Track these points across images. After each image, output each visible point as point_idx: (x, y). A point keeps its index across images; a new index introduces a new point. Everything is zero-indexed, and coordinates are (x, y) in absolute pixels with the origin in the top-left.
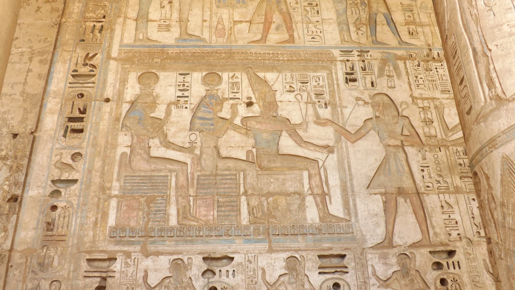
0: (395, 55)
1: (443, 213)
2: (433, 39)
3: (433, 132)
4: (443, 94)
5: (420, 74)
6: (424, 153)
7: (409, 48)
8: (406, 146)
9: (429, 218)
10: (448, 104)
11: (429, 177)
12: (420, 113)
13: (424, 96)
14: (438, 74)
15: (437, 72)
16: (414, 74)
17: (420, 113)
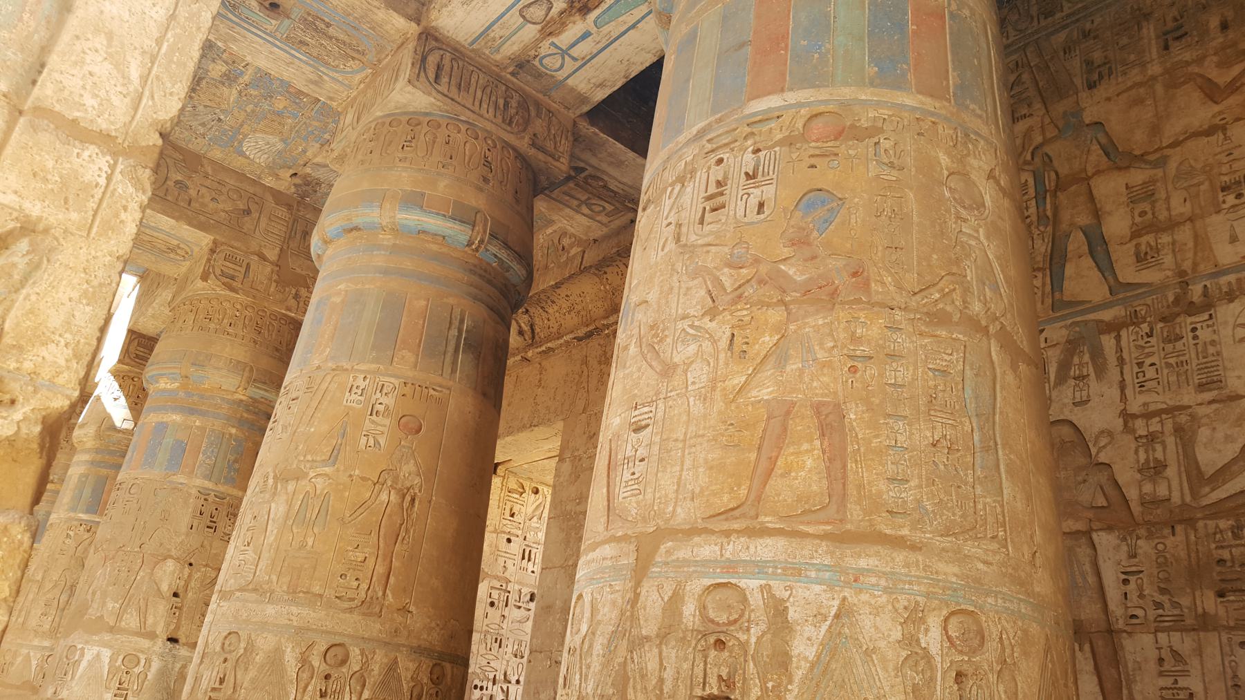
0: (1099, 322)
1: (1161, 674)
2: (1195, 254)
3: (1162, 491)
4: (1202, 391)
5: (1149, 355)
6: (1134, 541)
7: (1131, 297)
8: (1096, 530)
9: (1127, 684)
10: (1212, 415)
11: (1138, 597)
12: (1136, 452)
13: (1152, 408)
14: (1196, 345)
15: (1195, 337)
16: (1136, 358)
17: (1136, 452)
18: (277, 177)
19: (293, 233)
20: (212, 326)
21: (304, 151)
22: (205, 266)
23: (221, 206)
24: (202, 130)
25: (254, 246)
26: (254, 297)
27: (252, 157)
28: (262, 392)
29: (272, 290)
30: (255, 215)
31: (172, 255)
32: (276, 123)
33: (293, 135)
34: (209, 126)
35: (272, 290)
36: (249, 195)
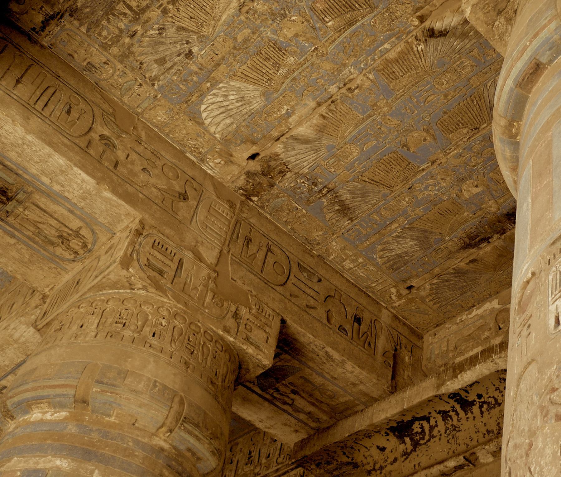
18: (229, 158)
19: (235, 236)
20: (127, 333)
21: (289, 115)
22: (127, 249)
23: (153, 181)
24: (155, 70)
25: (189, 239)
26: (186, 305)
27: (207, 122)
28: (192, 440)
29: (208, 300)
30: (192, 203)
31: (59, 251)
32: (269, 64)
33: (284, 85)
34: (168, 65)
35: (208, 300)
36: (188, 177)
